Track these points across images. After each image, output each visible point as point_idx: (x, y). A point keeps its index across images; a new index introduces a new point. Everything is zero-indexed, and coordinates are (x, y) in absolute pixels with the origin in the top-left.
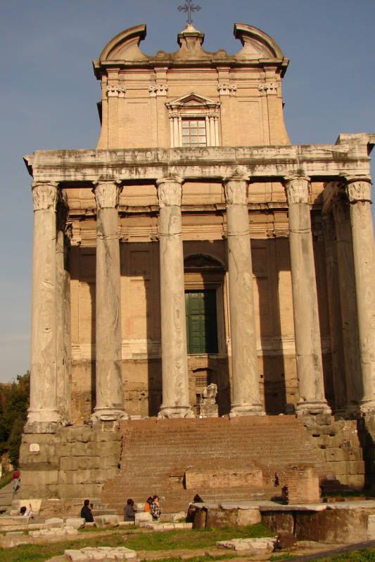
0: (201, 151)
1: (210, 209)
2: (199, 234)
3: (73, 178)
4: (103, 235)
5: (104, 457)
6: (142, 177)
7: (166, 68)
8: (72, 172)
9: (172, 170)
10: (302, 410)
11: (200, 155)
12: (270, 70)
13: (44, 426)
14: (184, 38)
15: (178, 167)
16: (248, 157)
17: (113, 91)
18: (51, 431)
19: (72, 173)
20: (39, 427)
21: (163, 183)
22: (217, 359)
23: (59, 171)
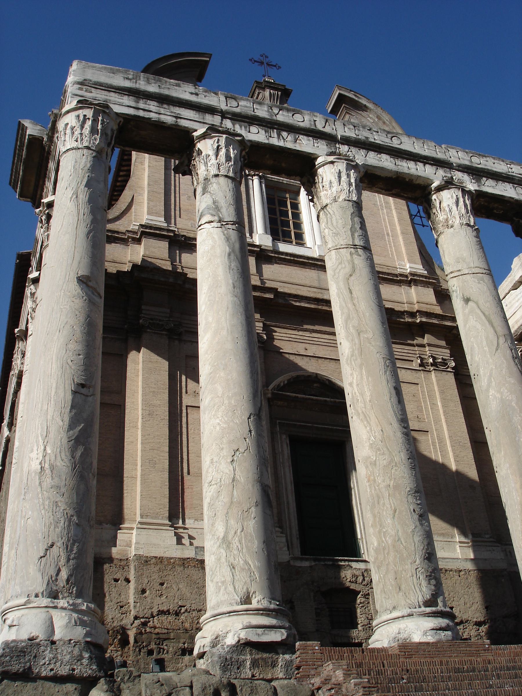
0: (390, 136)
2: (307, 346)
3: (153, 116)
6: (289, 145)
8: (152, 105)
9: (344, 149)
13: (65, 654)
15: (354, 150)
16: (467, 163)
20: (48, 655)
21: (332, 163)
22: (366, 570)
23: (126, 97)
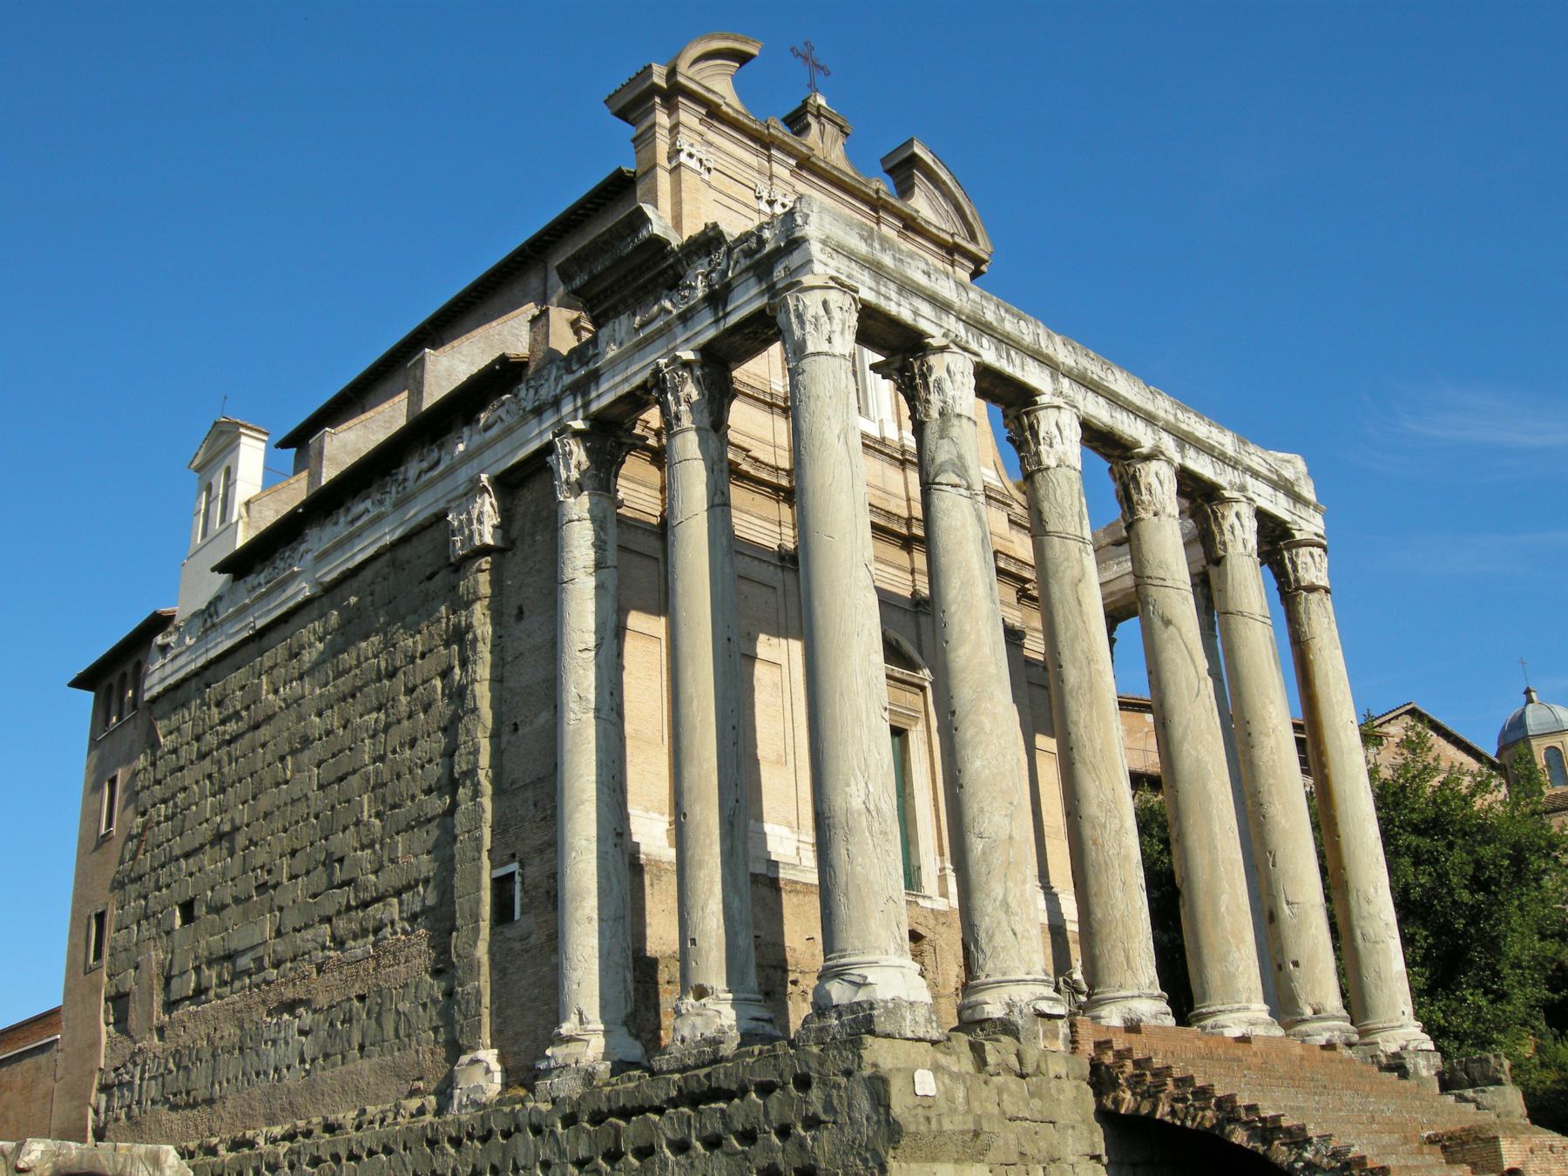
1: (896, 527)
4: (968, 488)
5: (1066, 1127)
7: (793, 162)
10: (1327, 1035)
11: (1102, 375)
12: (962, 266)
14: (818, 116)
17: (691, 156)
18: (935, 1035)
19: (894, 296)
21: (1059, 408)
23: (866, 273)
